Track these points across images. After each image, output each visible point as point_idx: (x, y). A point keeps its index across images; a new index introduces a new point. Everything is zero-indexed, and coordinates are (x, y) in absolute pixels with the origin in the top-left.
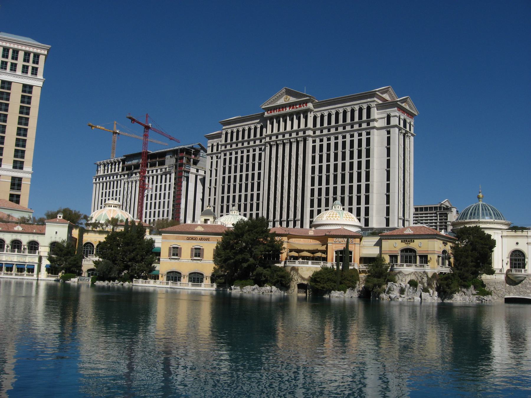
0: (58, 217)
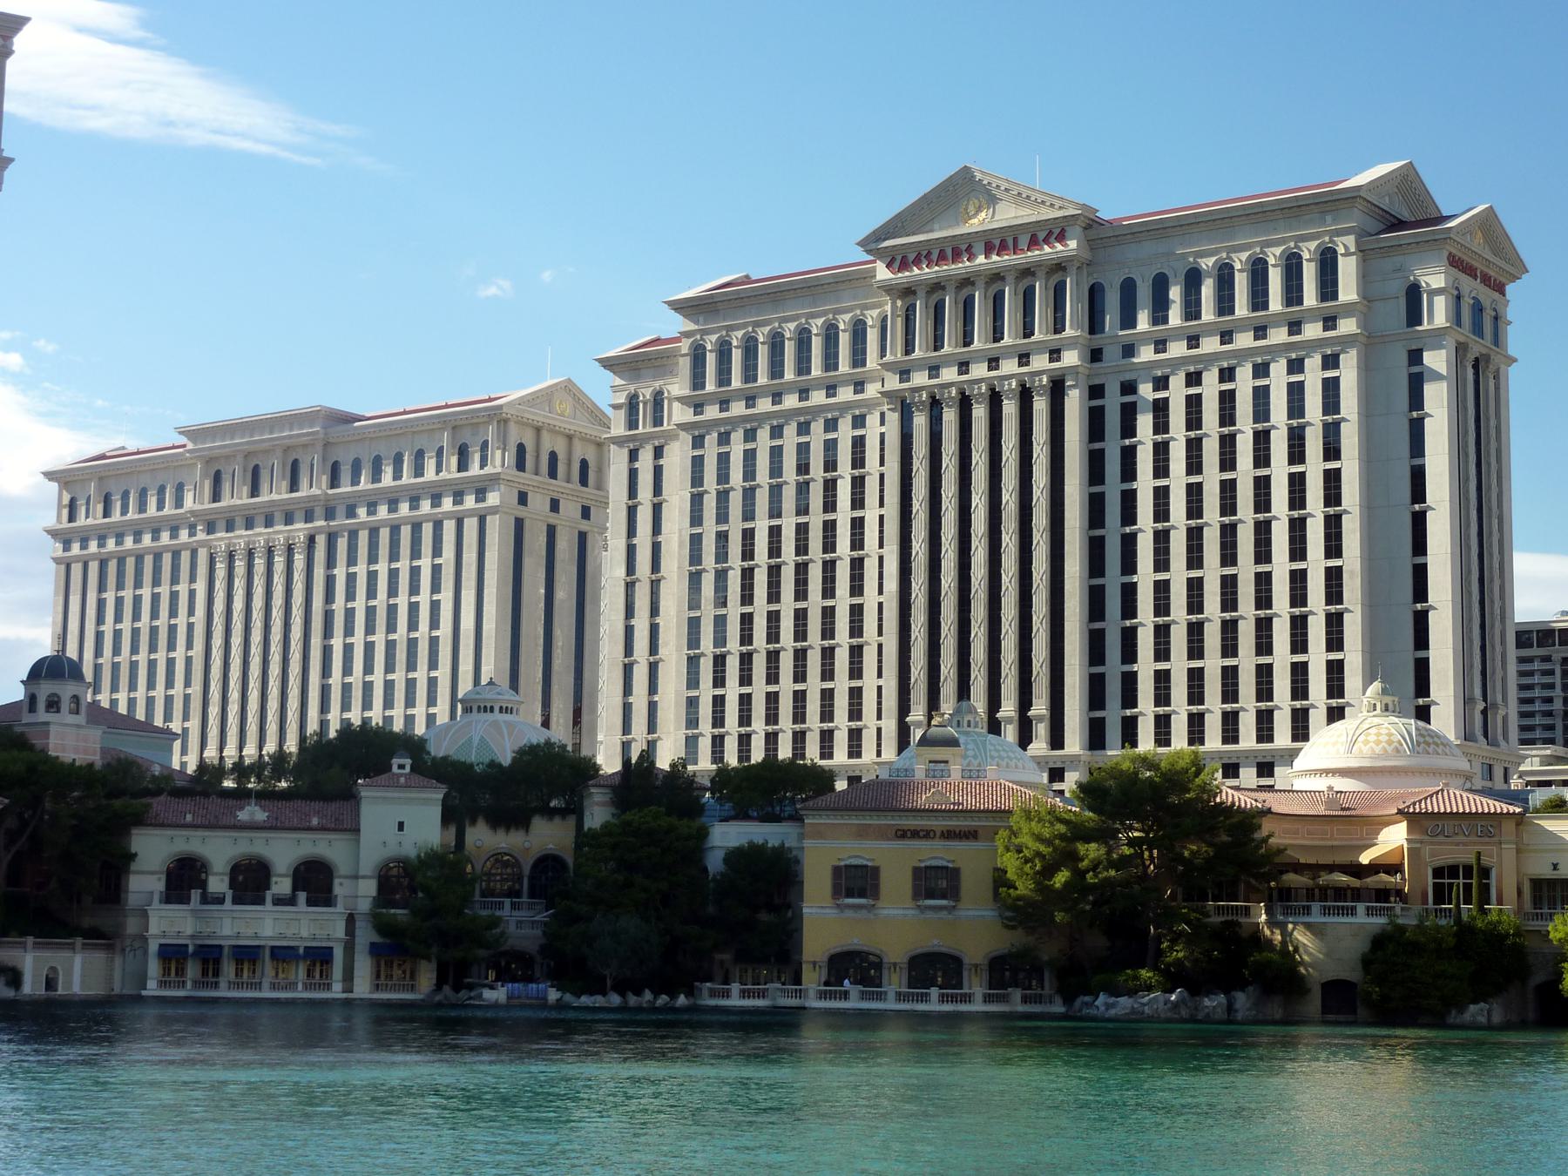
0: (395, 769)
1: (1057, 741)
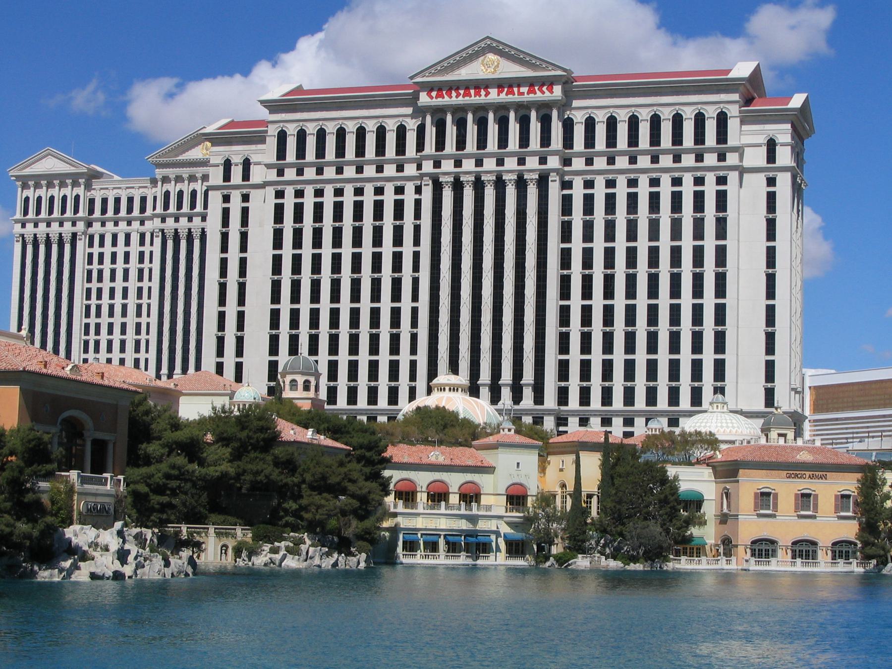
1: (539, 398)
